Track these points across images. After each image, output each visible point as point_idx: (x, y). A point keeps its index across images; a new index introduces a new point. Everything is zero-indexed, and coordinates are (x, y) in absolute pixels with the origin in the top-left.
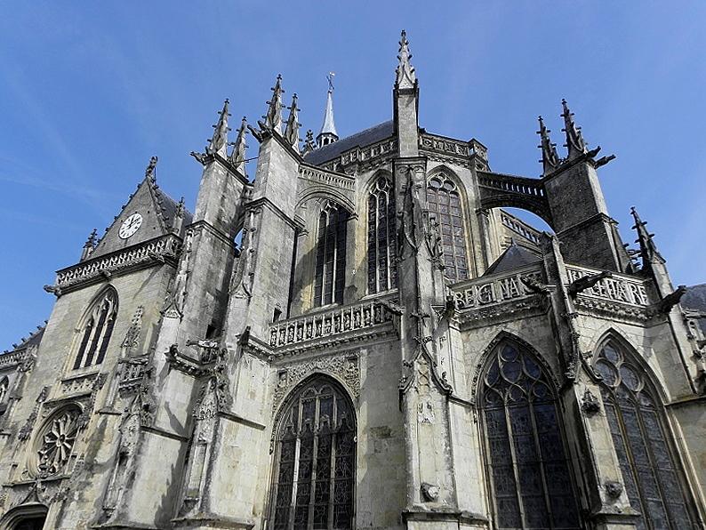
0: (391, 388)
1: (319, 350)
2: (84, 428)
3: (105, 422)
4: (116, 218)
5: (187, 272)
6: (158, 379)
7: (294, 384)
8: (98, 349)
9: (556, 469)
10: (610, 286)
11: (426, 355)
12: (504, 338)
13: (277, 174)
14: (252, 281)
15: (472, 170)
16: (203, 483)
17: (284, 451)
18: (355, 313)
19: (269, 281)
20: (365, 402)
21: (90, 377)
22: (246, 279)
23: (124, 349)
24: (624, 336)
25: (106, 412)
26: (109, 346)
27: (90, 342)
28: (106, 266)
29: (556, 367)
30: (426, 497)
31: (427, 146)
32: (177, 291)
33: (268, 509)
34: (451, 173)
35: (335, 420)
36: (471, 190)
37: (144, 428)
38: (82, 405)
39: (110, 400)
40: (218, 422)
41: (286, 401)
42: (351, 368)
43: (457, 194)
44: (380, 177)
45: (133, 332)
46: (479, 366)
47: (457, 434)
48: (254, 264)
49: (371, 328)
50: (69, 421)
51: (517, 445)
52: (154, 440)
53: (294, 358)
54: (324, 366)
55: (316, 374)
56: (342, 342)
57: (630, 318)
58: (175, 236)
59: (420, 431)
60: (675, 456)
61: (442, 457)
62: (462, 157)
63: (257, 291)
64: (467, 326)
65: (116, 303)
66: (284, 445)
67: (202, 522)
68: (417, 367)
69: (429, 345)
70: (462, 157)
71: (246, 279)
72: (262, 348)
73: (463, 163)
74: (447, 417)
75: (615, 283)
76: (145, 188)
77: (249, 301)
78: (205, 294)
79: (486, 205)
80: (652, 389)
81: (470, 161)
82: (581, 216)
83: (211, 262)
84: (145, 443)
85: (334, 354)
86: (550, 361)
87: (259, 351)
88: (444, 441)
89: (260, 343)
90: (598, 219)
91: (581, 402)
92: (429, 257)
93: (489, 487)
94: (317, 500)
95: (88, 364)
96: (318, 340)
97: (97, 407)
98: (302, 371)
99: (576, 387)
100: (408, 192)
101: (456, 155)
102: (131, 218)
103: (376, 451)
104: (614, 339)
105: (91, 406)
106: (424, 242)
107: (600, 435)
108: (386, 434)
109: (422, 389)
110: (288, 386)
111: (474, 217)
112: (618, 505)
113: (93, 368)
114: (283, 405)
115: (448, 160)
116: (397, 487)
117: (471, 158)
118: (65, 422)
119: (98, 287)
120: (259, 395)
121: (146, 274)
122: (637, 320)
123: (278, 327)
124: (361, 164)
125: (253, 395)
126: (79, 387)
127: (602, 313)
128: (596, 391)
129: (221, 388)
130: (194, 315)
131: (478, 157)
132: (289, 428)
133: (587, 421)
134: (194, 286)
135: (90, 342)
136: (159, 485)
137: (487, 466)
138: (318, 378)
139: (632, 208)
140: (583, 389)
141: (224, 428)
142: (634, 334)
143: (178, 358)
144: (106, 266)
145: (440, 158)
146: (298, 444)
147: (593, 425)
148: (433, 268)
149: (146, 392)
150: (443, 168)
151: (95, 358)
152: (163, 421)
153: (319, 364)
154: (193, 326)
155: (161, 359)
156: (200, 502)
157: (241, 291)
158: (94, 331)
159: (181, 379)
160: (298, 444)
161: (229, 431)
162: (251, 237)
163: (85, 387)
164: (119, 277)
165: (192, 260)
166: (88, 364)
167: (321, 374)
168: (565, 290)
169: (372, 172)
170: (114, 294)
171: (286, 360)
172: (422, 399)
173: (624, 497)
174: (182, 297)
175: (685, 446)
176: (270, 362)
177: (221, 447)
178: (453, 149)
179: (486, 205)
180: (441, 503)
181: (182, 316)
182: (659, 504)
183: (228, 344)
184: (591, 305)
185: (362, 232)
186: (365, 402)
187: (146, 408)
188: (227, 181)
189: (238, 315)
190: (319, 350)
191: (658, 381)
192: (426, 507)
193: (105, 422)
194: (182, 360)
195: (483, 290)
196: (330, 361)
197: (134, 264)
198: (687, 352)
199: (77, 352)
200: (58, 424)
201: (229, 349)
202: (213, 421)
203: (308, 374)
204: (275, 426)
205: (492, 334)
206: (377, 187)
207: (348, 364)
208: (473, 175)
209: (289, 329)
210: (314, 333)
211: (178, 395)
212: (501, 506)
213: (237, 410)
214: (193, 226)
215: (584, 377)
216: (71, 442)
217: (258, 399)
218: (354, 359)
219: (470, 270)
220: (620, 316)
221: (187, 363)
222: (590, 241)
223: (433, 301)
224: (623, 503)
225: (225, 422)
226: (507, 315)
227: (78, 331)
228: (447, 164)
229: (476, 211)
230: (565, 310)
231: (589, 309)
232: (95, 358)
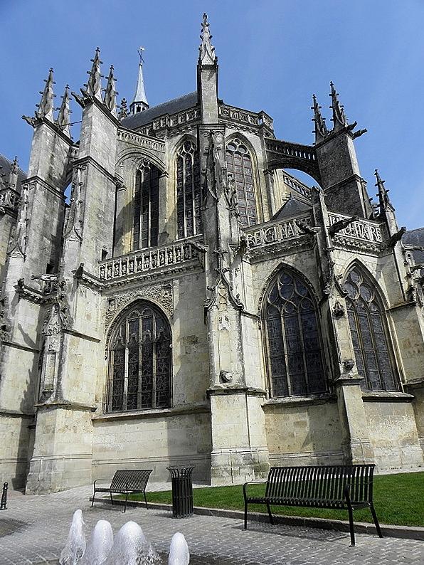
0: (197, 308)
1: (140, 282)
5: (26, 220)
6: (10, 306)
7: (121, 308)
9: (313, 356)
10: (358, 228)
11: (224, 282)
12: (283, 268)
13: (99, 136)
14: (82, 227)
16: (56, 380)
17: (116, 356)
18: (168, 252)
19: (96, 227)
20: (178, 319)
22: (77, 226)
29: (318, 288)
30: (224, 380)
31: (225, 116)
33: (107, 397)
34: (245, 139)
35: (155, 333)
36: (260, 154)
40: (63, 337)
42: (166, 294)
43: (249, 157)
44: (186, 141)
46: (264, 289)
48: (83, 213)
49: (182, 264)
51: (288, 342)
53: (121, 289)
54: (145, 294)
55: (139, 300)
56: (158, 275)
57: (369, 251)
59: (220, 336)
60: (389, 342)
61: (235, 353)
62: (254, 126)
63: (87, 235)
64: (255, 260)
66: (116, 353)
67: (58, 406)
68: (218, 291)
69: (227, 274)
70: (254, 126)
71: (77, 226)
72: (93, 281)
74: (240, 325)
75: (361, 226)
78: (42, 239)
79: (272, 166)
80: (379, 300)
81: (260, 130)
82: (341, 176)
83: (46, 212)
84: (6, 354)
85: (153, 284)
86: (314, 283)
87: (92, 283)
88: (237, 342)
89: (92, 277)
90: (353, 179)
91: (332, 309)
92: (228, 207)
93: (268, 371)
94: (143, 389)
98: (126, 298)
99: (330, 299)
100: (210, 153)
101: (249, 124)
103: (186, 353)
104: (358, 267)
106: (223, 194)
107: (343, 331)
108: (194, 340)
109: (222, 307)
111: (262, 176)
112: (351, 374)
115: (242, 128)
116: (202, 376)
117: (260, 127)
120: (94, 316)
122: (374, 253)
124: (170, 129)
125: (89, 317)
127: (351, 247)
128: (343, 302)
129: (63, 311)
130: (35, 255)
131: (265, 126)
132: (119, 341)
133: (335, 322)
136: (20, 384)
137: (267, 358)
138: (140, 303)
139: (376, 170)
140: (335, 300)
141: (68, 340)
142: (370, 262)
143: (25, 290)
145: (235, 126)
146: (127, 352)
147: (339, 324)
148: (231, 216)
150: (237, 135)
152: (18, 338)
153: (141, 292)
154: (34, 264)
155: (11, 290)
156: (54, 393)
157: (74, 235)
159: (29, 306)
160: (127, 352)
161: (72, 344)
162: (79, 191)
165: (29, 210)
167: (143, 300)
168: (327, 231)
169: (180, 136)
171: (114, 290)
172: (221, 314)
173: (355, 369)
174: (23, 241)
175: (396, 336)
176: (101, 292)
177: (67, 354)
178: (246, 118)
179: (272, 166)
180: (232, 385)
181: (25, 256)
182: (376, 372)
183: (65, 278)
185: (172, 188)
186: (178, 319)
188: (54, 142)
189: (73, 254)
190: (140, 282)
191: (383, 294)
192: (223, 386)
194: (28, 291)
195: (268, 232)
196: (150, 290)
198: (403, 274)
201: (67, 282)
202: (59, 336)
203: (132, 300)
204: (108, 340)
206: (184, 149)
208: (262, 141)
209: (115, 265)
210: (136, 269)
212: (275, 383)
213: (77, 327)
215: (336, 292)
217: (93, 320)
218: (169, 288)
219: (259, 219)
220: (363, 250)
222: (347, 195)
223: (230, 240)
224: (354, 373)
225: (68, 337)
228: (241, 132)
229: (264, 172)
230: (326, 245)
231: (342, 245)
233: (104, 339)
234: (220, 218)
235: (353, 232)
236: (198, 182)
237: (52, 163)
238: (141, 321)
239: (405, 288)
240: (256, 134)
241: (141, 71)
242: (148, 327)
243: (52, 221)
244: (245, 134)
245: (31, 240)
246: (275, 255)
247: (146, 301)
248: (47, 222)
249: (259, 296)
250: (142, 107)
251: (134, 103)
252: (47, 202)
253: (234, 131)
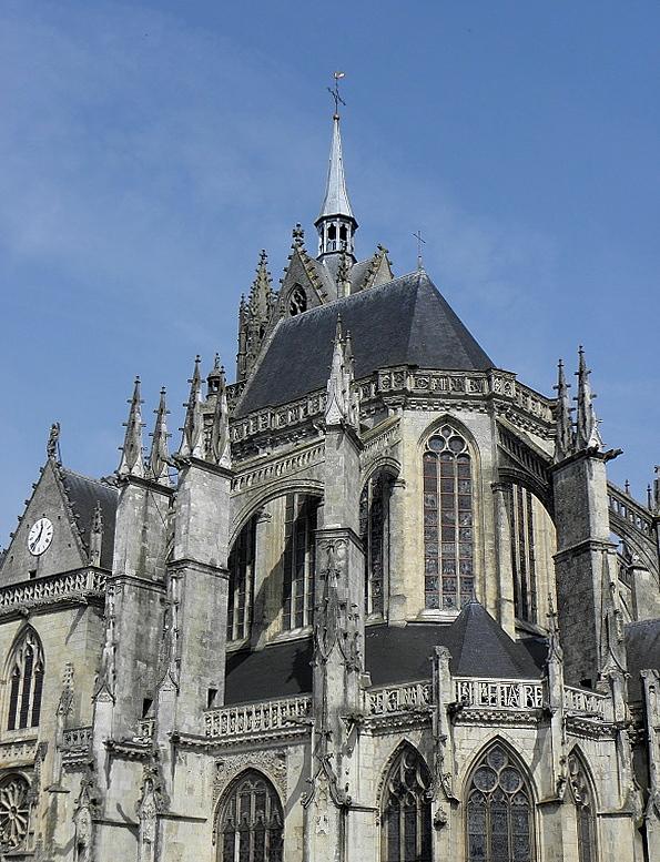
1: (250, 745)
2: (35, 804)
3: (55, 799)
4: (20, 519)
5: (113, 644)
7: (231, 777)
8: (31, 708)
10: (503, 693)
12: (405, 745)
14: (178, 666)
15: (491, 414)
21: (31, 742)
23: (60, 717)
24: (509, 740)
25: (55, 790)
26: (42, 709)
27: (20, 698)
28: (21, 599)
32: (106, 669)
34: (459, 424)
35: (268, 816)
37: (95, 822)
38: (28, 776)
39: (56, 775)
40: (158, 823)
43: (468, 457)
45: (67, 697)
46: (385, 772)
47: (355, 839)
48: (180, 646)
50: (17, 791)
52: (105, 830)
53: (230, 750)
54: (258, 760)
55: (250, 768)
57: (520, 722)
58: (95, 569)
63: (186, 676)
64: (378, 731)
65: (40, 647)
66: (226, 836)
68: (318, 783)
72: (194, 741)
73: (477, 407)
76: (49, 474)
77: (178, 691)
79: (505, 479)
80: (526, 792)
83: (139, 623)
84: (98, 835)
85: (266, 750)
89: (192, 737)
91: (433, 817)
95: (23, 725)
96: (249, 734)
97: (44, 782)
98: (237, 763)
101: (466, 397)
102: (39, 523)
104: (500, 747)
105: (37, 780)
110: (226, 779)
111: (488, 495)
113: (30, 732)
115: (453, 406)
117: (488, 398)
118: (13, 792)
119: (17, 624)
120: (197, 788)
121: (69, 616)
122: (529, 723)
123: (211, 714)
125: (191, 790)
126: (19, 753)
127: (490, 721)
129: (158, 790)
130: (127, 692)
133: (434, 832)
134: (123, 659)
135: (20, 698)
138: (251, 773)
141: (165, 827)
142: (522, 739)
144: (21, 599)
147: (439, 836)
148: (348, 669)
149: (92, 786)
150: (447, 418)
151: (30, 719)
152: (111, 813)
153: (252, 758)
154: (126, 706)
157: (168, 683)
158: (21, 683)
159: (122, 767)
160: (238, 836)
161: (169, 830)
162: (174, 610)
163: (26, 755)
164: (39, 615)
165: (117, 627)
166: (23, 725)
167: (254, 769)
170: (35, 635)
174: (111, 676)
177: (163, 845)
178: (461, 386)
181: (114, 699)
183: (160, 743)
184: (477, 717)
187: (94, 802)
188: (146, 504)
190: (250, 745)
193: (55, 799)
195: (391, 697)
199: (7, 709)
200: (5, 794)
201: (161, 748)
203: (243, 768)
211: (121, 782)
213: (175, 809)
214: (114, 579)
215: (442, 796)
216: (25, 815)
217: (197, 792)
218: (283, 757)
219: (478, 578)
220: (509, 722)
221: (126, 750)
222: (580, 573)
223: (342, 709)
225: (165, 823)
226: (406, 725)
227: (4, 682)
228: (454, 413)
229: (492, 486)
231: (475, 720)
232: (30, 719)
233: (210, 816)
234: (329, 682)
235: (493, 700)
236: (377, 516)
237: (144, 540)
238: (253, 797)
239: (557, 773)
240: (482, 411)
241: (336, 133)
242: (262, 806)
243: (148, 632)
244: (460, 415)
245: (121, 673)
246: (398, 729)
248: (141, 636)
249: (379, 780)
250: (338, 225)
251: (323, 219)
252: (140, 607)
253: (438, 414)
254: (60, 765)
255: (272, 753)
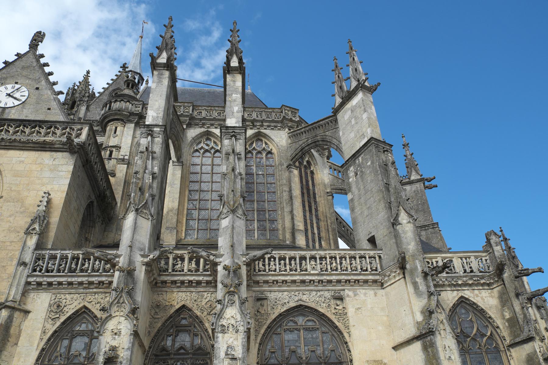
0: (380, 328)
29: (504, 328)
41: (268, 327)
55: (301, 305)
85: (319, 291)
114: (266, 330)
139: (500, 228)
153: (301, 296)
193: (10, 319)
197: (28, 142)
203: (292, 304)
204: (259, 350)
205: (455, 297)
207: (333, 302)
218: (341, 299)
247: (312, 308)
254: (23, 282)
255: (327, 294)
